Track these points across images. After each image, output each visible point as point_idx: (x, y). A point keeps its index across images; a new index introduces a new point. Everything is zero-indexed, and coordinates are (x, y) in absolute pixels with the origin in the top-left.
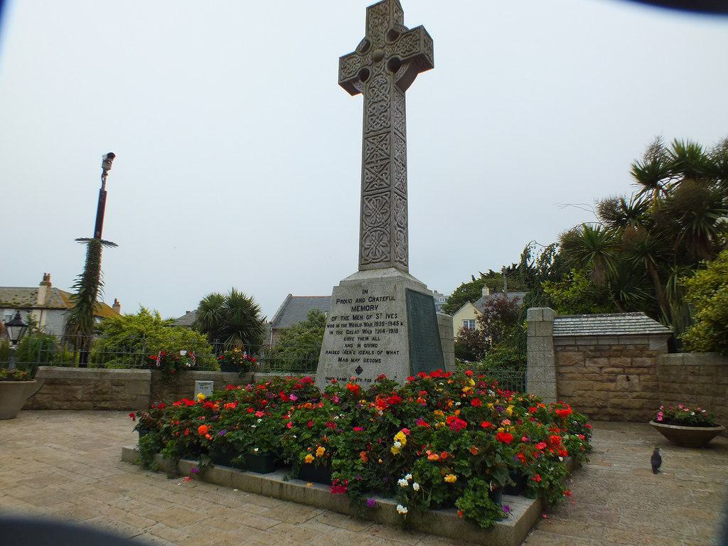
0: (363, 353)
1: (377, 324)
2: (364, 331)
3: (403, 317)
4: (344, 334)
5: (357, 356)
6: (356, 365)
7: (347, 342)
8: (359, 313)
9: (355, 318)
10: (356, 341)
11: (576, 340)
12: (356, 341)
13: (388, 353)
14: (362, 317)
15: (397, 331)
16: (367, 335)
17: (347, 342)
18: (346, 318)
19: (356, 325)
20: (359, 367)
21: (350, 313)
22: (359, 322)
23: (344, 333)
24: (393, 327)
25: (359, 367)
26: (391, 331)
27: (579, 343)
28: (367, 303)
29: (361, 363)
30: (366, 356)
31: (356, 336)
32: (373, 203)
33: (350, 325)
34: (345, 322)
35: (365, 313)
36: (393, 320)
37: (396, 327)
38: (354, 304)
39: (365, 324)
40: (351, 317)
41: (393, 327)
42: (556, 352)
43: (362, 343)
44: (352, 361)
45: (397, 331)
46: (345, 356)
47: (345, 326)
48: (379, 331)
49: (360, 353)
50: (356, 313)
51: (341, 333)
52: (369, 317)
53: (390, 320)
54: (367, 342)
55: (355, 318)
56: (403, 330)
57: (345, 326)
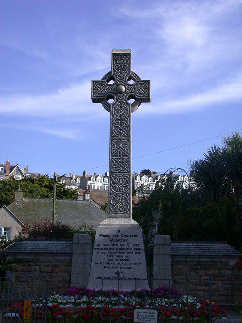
0: (118, 264)
2: (120, 253)
3: (142, 246)
4: (107, 254)
5: (116, 266)
6: (116, 270)
7: (109, 258)
8: (116, 243)
9: (113, 245)
10: (115, 258)
11: (199, 258)
12: (115, 258)
13: (135, 264)
14: (117, 245)
15: (140, 253)
16: (121, 255)
17: (109, 258)
18: (108, 245)
21: (110, 243)
22: (116, 248)
23: (107, 253)
24: (137, 251)
26: (137, 253)
27: (187, 260)
28: (120, 237)
29: (119, 269)
30: (122, 266)
31: (115, 255)
32: (118, 180)
33: (110, 249)
34: (107, 247)
36: (137, 248)
38: (112, 237)
39: (120, 249)
40: (110, 246)
41: (137, 251)
42: (172, 265)
43: (119, 259)
45: (140, 253)
46: (107, 266)
47: (107, 249)
49: (118, 264)
50: (113, 243)
51: (104, 253)
52: (122, 245)
53: (135, 247)
55: (113, 245)
56: (143, 253)
57: (107, 249)
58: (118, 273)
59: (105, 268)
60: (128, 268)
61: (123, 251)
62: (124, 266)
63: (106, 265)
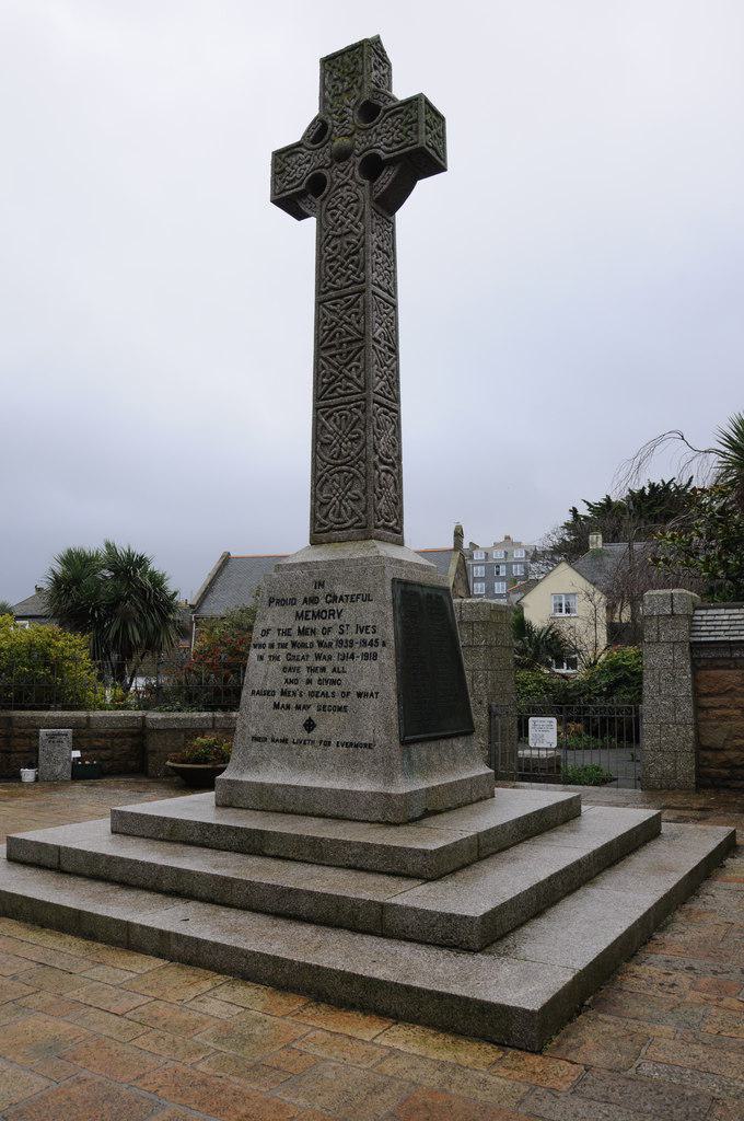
0: (312, 694)
1: (340, 643)
6: (303, 716)
13: (359, 695)
15: (375, 657)
17: (291, 676)
18: (287, 632)
19: (304, 645)
20: (310, 720)
23: (283, 658)
24: (367, 650)
25: (310, 720)
26: (366, 656)
29: (313, 713)
31: (303, 664)
33: (294, 644)
35: (318, 624)
37: (374, 649)
41: (367, 650)
43: (315, 677)
44: (298, 707)
45: (375, 657)
47: (284, 646)
48: (344, 657)
54: (323, 676)
57: (284, 646)
58: (310, 725)
59: (276, 706)
60: (340, 709)
61: (326, 652)
62: (329, 702)
63: (277, 698)
